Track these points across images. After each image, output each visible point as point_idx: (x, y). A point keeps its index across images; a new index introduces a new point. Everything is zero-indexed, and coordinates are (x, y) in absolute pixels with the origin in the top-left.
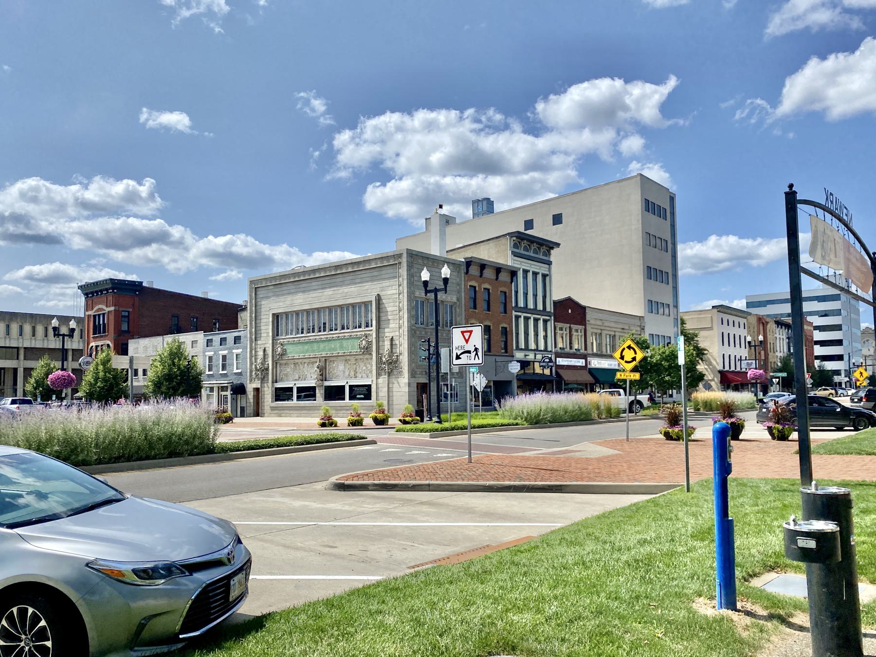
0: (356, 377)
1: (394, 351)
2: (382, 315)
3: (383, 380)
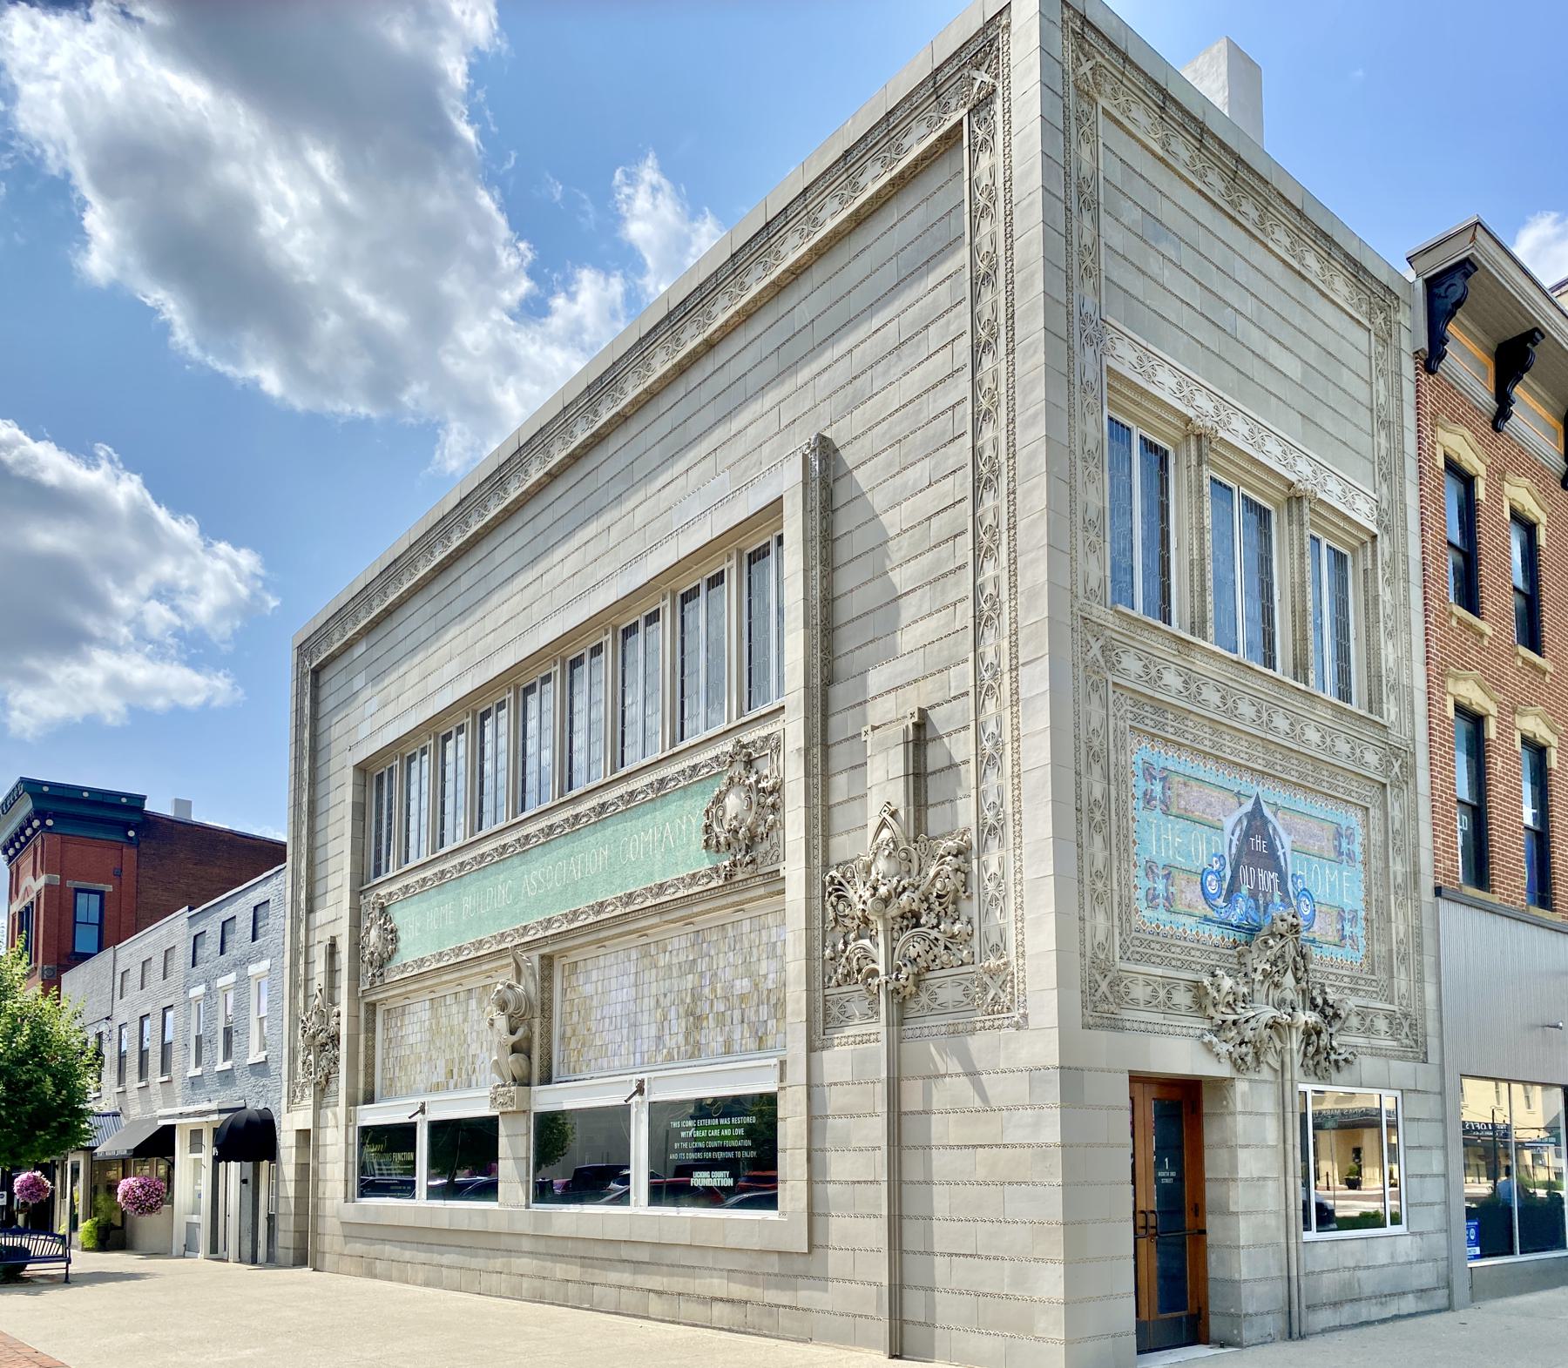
0: (695, 1051)
2: (846, 580)
3: (859, 1050)
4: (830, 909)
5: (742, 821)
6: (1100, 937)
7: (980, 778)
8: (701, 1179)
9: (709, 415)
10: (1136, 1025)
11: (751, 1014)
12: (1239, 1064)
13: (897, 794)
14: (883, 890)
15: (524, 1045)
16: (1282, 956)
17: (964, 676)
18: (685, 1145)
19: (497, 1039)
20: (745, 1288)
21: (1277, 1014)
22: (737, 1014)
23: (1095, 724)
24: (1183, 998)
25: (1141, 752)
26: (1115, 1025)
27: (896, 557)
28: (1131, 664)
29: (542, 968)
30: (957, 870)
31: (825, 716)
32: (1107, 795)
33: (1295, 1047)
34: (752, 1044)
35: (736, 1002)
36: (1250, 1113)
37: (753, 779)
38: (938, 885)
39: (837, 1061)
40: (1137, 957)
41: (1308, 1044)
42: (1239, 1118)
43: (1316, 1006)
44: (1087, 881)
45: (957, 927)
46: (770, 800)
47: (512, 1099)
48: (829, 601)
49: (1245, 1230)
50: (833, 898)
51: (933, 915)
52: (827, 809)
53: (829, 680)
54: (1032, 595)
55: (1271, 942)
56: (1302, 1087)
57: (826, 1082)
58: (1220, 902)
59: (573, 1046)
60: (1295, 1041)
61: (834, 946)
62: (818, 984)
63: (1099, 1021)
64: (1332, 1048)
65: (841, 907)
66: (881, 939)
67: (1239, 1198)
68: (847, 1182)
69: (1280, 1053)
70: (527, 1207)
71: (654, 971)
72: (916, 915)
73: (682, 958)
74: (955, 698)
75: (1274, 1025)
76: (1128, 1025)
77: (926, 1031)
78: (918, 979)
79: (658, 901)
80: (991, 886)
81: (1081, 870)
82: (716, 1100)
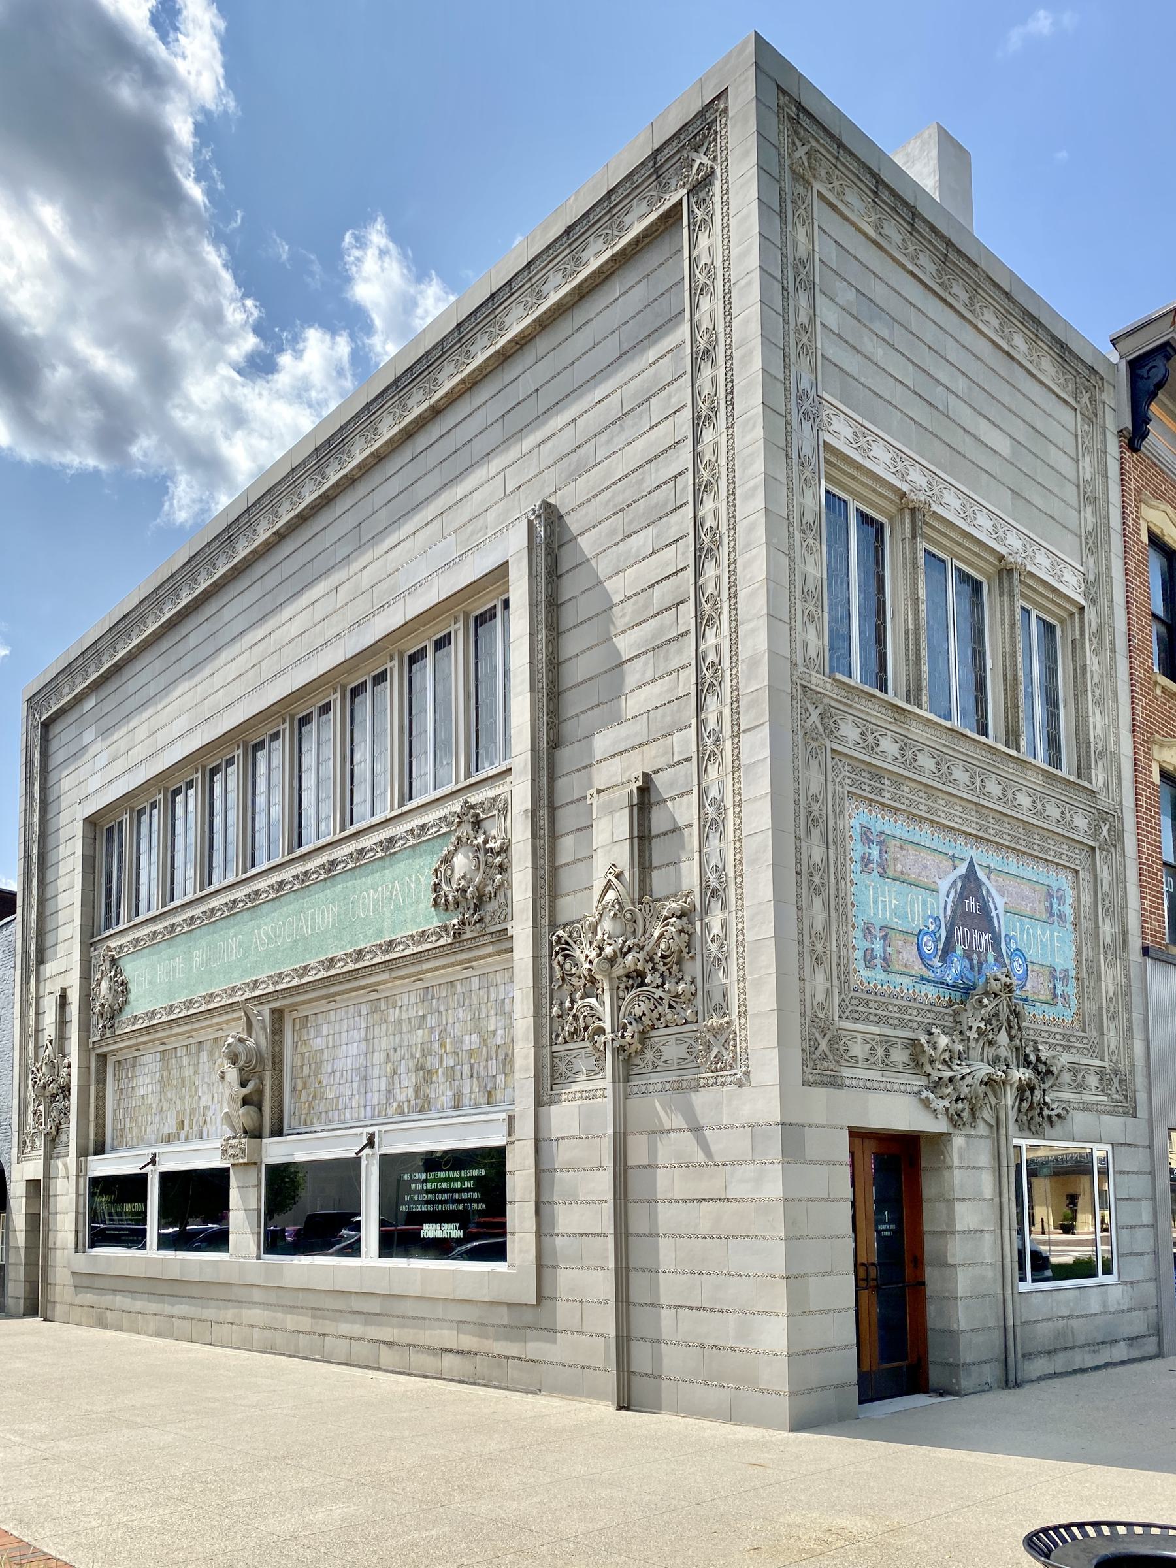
0: (425, 1105)
1: (659, 881)
2: (571, 645)
3: (585, 1107)
4: (557, 968)
5: (471, 881)
6: (820, 997)
7: (703, 841)
8: (430, 1231)
9: (434, 481)
10: (854, 1082)
11: (480, 1069)
12: (955, 1120)
13: (622, 856)
14: (608, 950)
15: (255, 1098)
16: (996, 1015)
17: (687, 742)
18: (415, 1197)
19: (227, 1092)
20: (475, 1339)
21: (992, 1070)
22: (466, 1069)
23: (814, 789)
24: (900, 1056)
25: (857, 817)
26: (834, 1082)
27: (621, 623)
28: (849, 731)
29: (273, 1021)
30: (681, 931)
31: (552, 779)
32: (826, 859)
33: (1009, 1103)
34: (481, 1098)
35: (465, 1056)
36: (968, 1167)
37: (481, 839)
38: (663, 946)
39: (565, 1116)
40: (856, 1015)
41: (1022, 1100)
42: (956, 1172)
43: (1029, 1063)
44: (807, 942)
45: (681, 987)
46: (498, 860)
47: (243, 1151)
48: (555, 665)
49: (963, 1282)
50: (560, 957)
51: (657, 975)
52: (554, 870)
53: (555, 744)
54: (754, 663)
55: (985, 1001)
56: (1016, 1142)
57: (554, 1135)
58: (936, 962)
59: (304, 1097)
60: (1010, 1098)
61: (561, 1004)
62: (546, 1040)
63: (819, 1079)
64: (1045, 1104)
65: (567, 966)
66: (607, 998)
67: (957, 1250)
68: (574, 1235)
69: (995, 1109)
70: (259, 1258)
71: (384, 1026)
72: (641, 975)
73: (412, 1013)
74: (678, 763)
75: (989, 1082)
76: (847, 1082)
77: (651, 1088)
78: (644, 1037)
79: (388, 958)
80: (714, 947)
81: (800, 932)
82: (446, 1152)
